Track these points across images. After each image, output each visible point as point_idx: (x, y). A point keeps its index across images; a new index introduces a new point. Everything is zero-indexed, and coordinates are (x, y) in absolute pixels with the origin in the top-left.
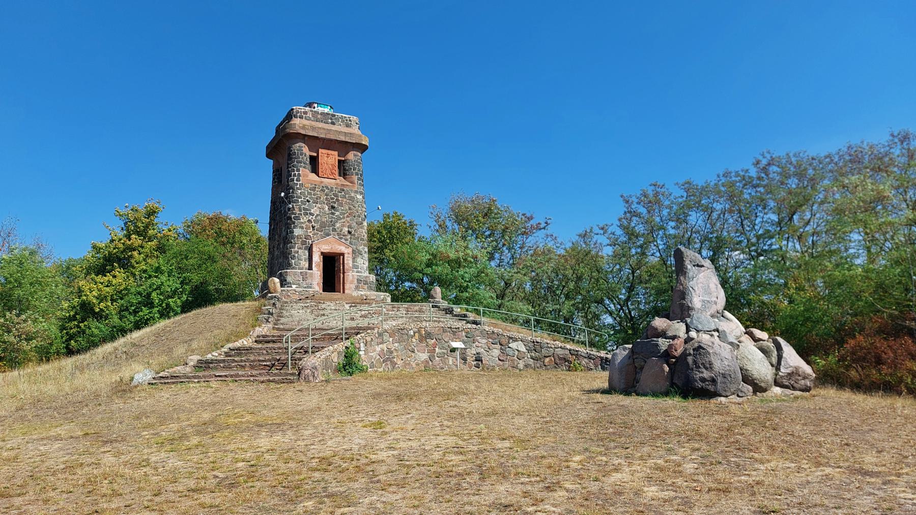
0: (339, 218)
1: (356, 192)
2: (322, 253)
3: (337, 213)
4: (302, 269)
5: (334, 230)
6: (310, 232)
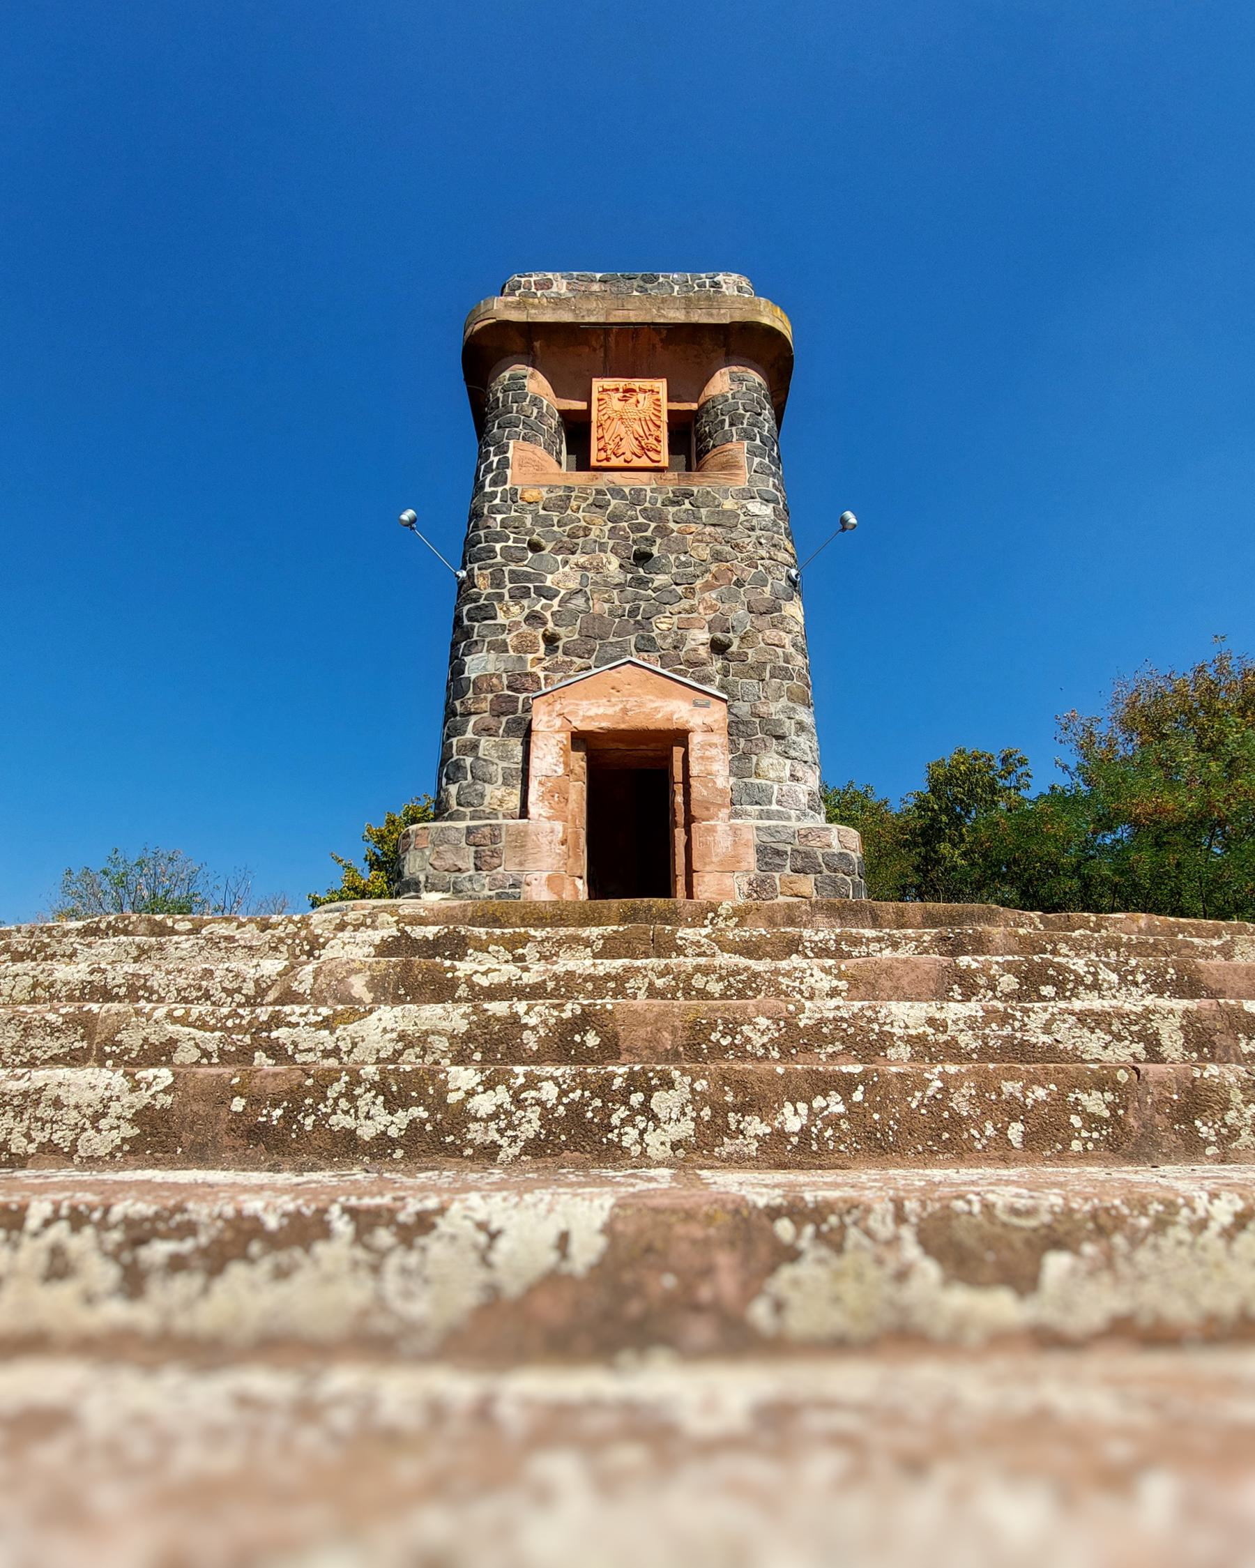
0: (664, 599)
3: (660, 579)
6: (536, 663)
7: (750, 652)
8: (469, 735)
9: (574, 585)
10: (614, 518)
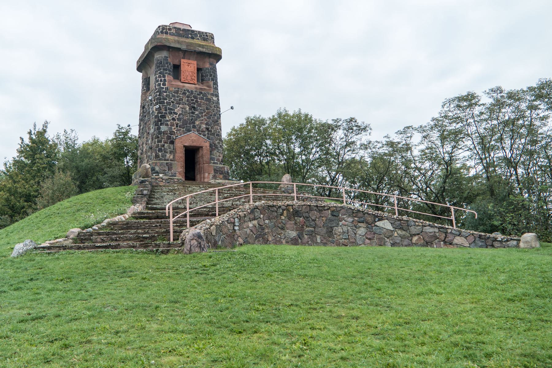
2: (184, 146)
3: (197, 113)
4: (168, 160)
5: (194, 127)
6: (174, 129)
8: (163, 143)
9: (180, 112)
10: (188, 97)
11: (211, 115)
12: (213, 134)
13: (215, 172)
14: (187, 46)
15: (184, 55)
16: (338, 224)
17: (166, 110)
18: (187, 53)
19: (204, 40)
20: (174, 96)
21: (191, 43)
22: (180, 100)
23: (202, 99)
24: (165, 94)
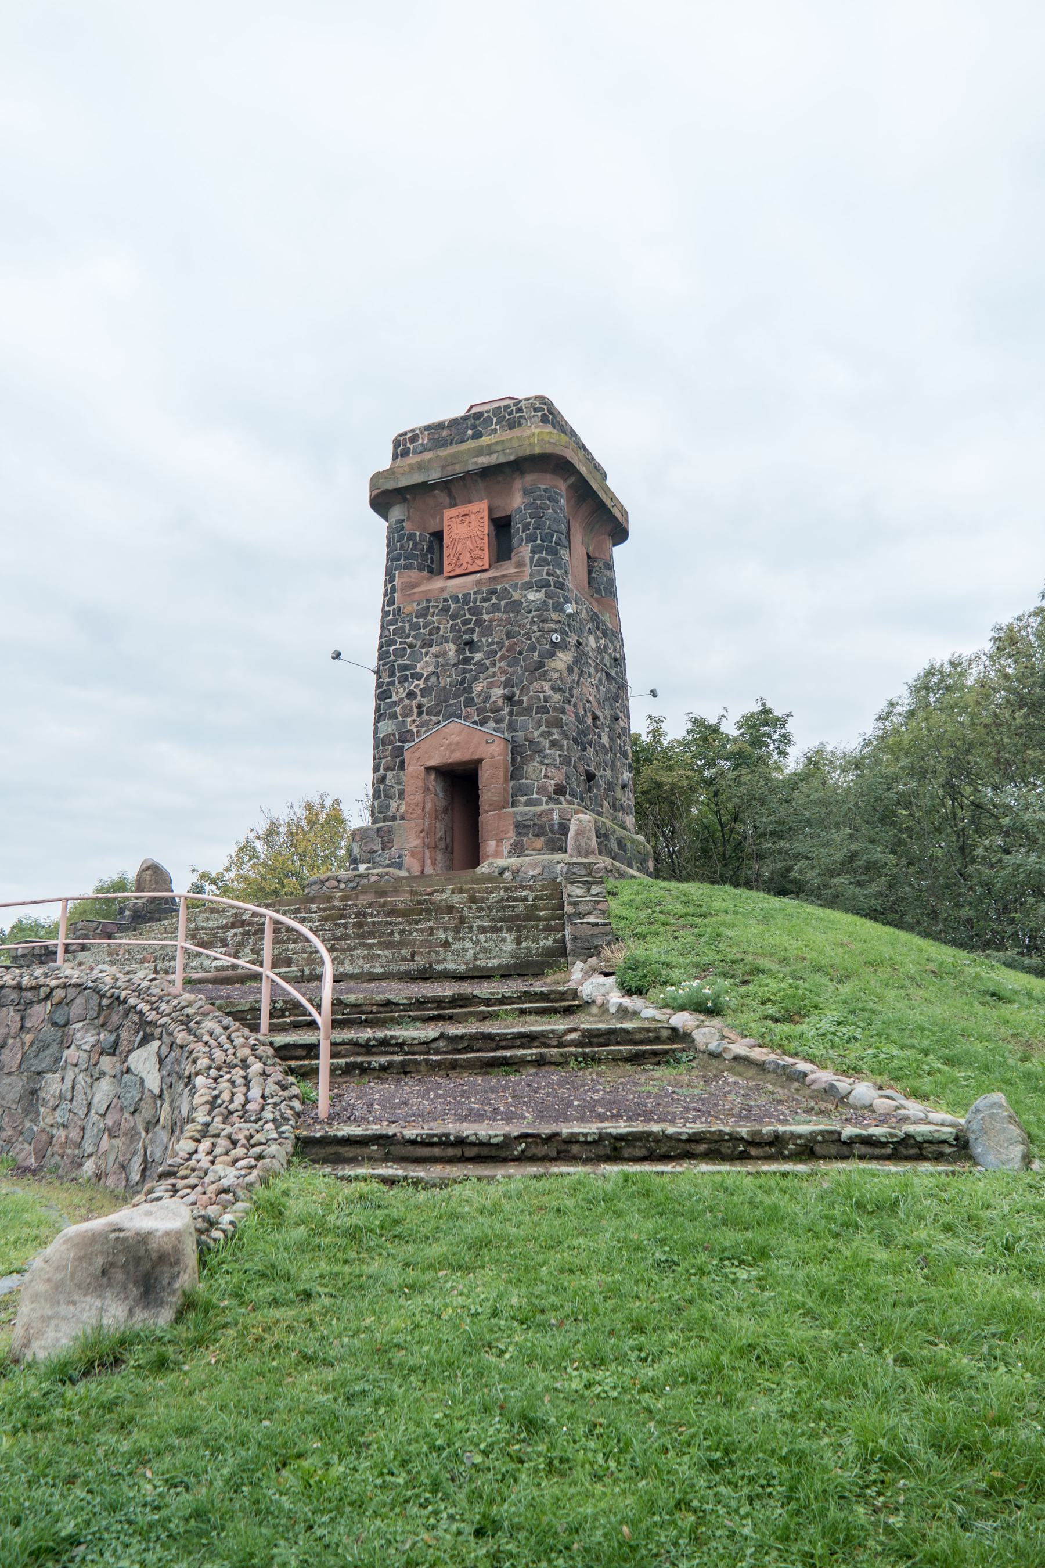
0: (482, 667)
1: (528, 586)
3: (478, 656)
4: (394, 818)
7: (525, 699)
9: (431, 669)
10: (454, 617)
11: (520, 653)
12: (527, 711)
13: (519, 834)
14: (444, 467)
15: (450, 494)
16: (57, 1060)
17: (392, 674)
18: (454, 487)
19: (512, 425)
20: (415, 627)
21: (454, 456)
22: (430, 634)
23: (495, 608)
24: (392, 628)
